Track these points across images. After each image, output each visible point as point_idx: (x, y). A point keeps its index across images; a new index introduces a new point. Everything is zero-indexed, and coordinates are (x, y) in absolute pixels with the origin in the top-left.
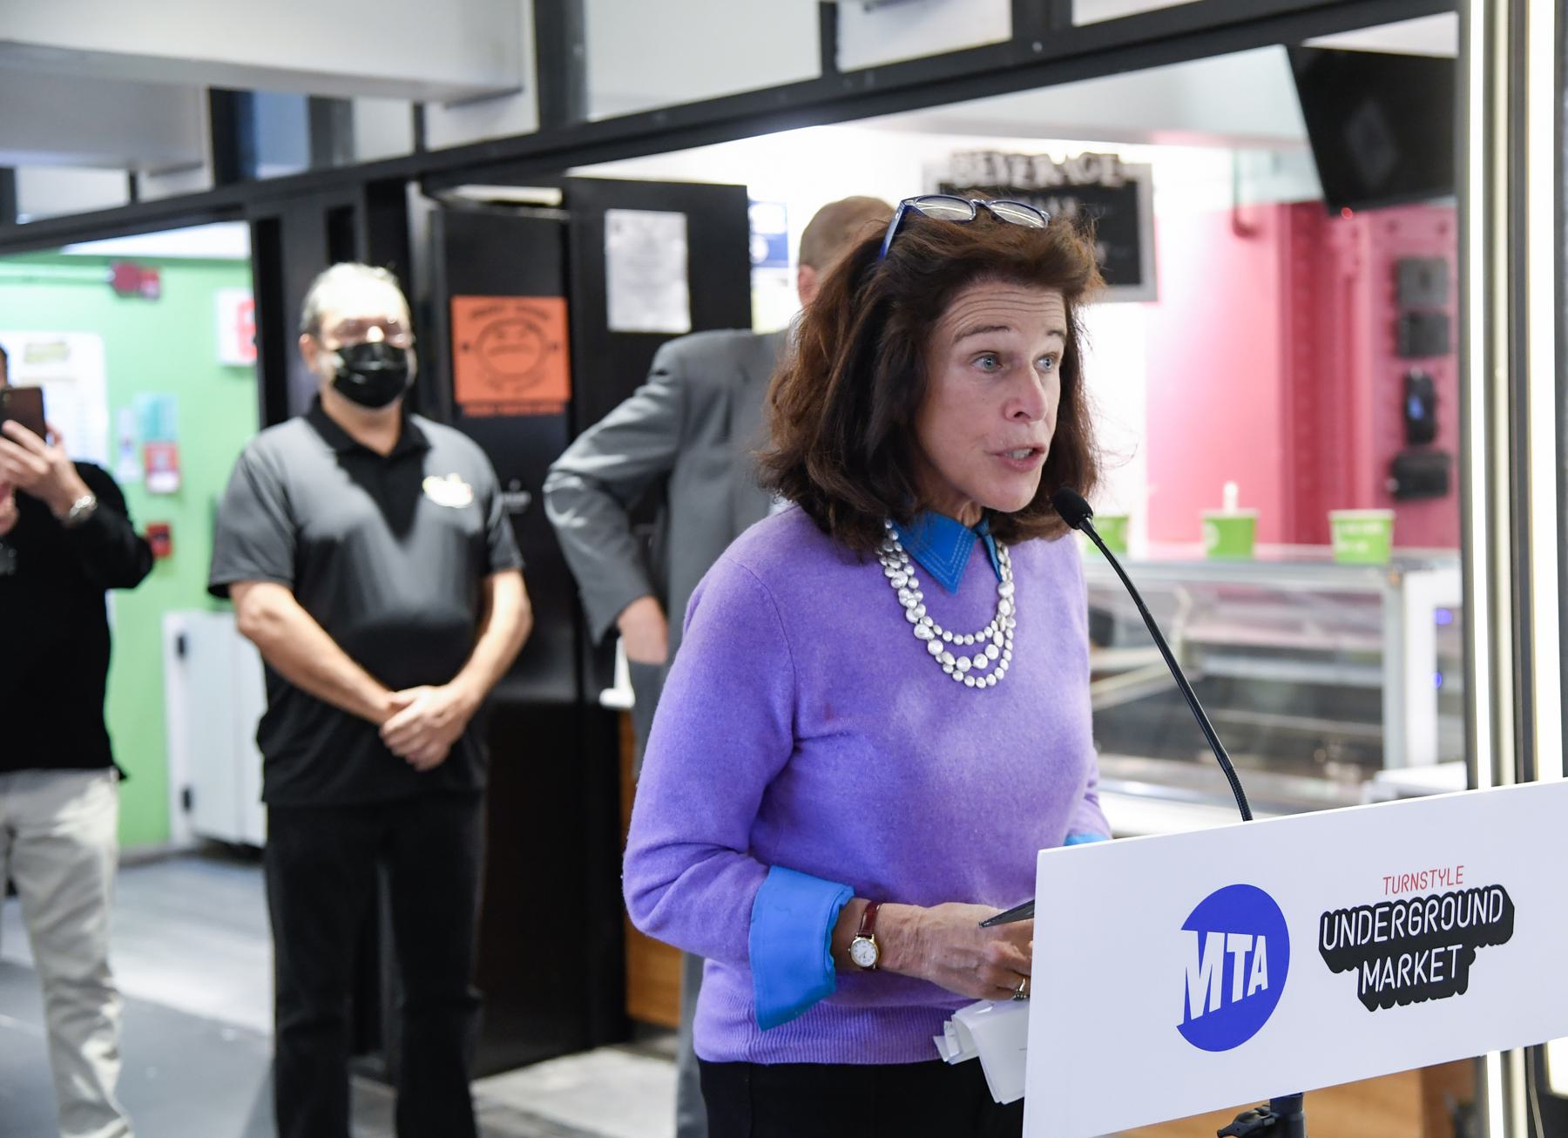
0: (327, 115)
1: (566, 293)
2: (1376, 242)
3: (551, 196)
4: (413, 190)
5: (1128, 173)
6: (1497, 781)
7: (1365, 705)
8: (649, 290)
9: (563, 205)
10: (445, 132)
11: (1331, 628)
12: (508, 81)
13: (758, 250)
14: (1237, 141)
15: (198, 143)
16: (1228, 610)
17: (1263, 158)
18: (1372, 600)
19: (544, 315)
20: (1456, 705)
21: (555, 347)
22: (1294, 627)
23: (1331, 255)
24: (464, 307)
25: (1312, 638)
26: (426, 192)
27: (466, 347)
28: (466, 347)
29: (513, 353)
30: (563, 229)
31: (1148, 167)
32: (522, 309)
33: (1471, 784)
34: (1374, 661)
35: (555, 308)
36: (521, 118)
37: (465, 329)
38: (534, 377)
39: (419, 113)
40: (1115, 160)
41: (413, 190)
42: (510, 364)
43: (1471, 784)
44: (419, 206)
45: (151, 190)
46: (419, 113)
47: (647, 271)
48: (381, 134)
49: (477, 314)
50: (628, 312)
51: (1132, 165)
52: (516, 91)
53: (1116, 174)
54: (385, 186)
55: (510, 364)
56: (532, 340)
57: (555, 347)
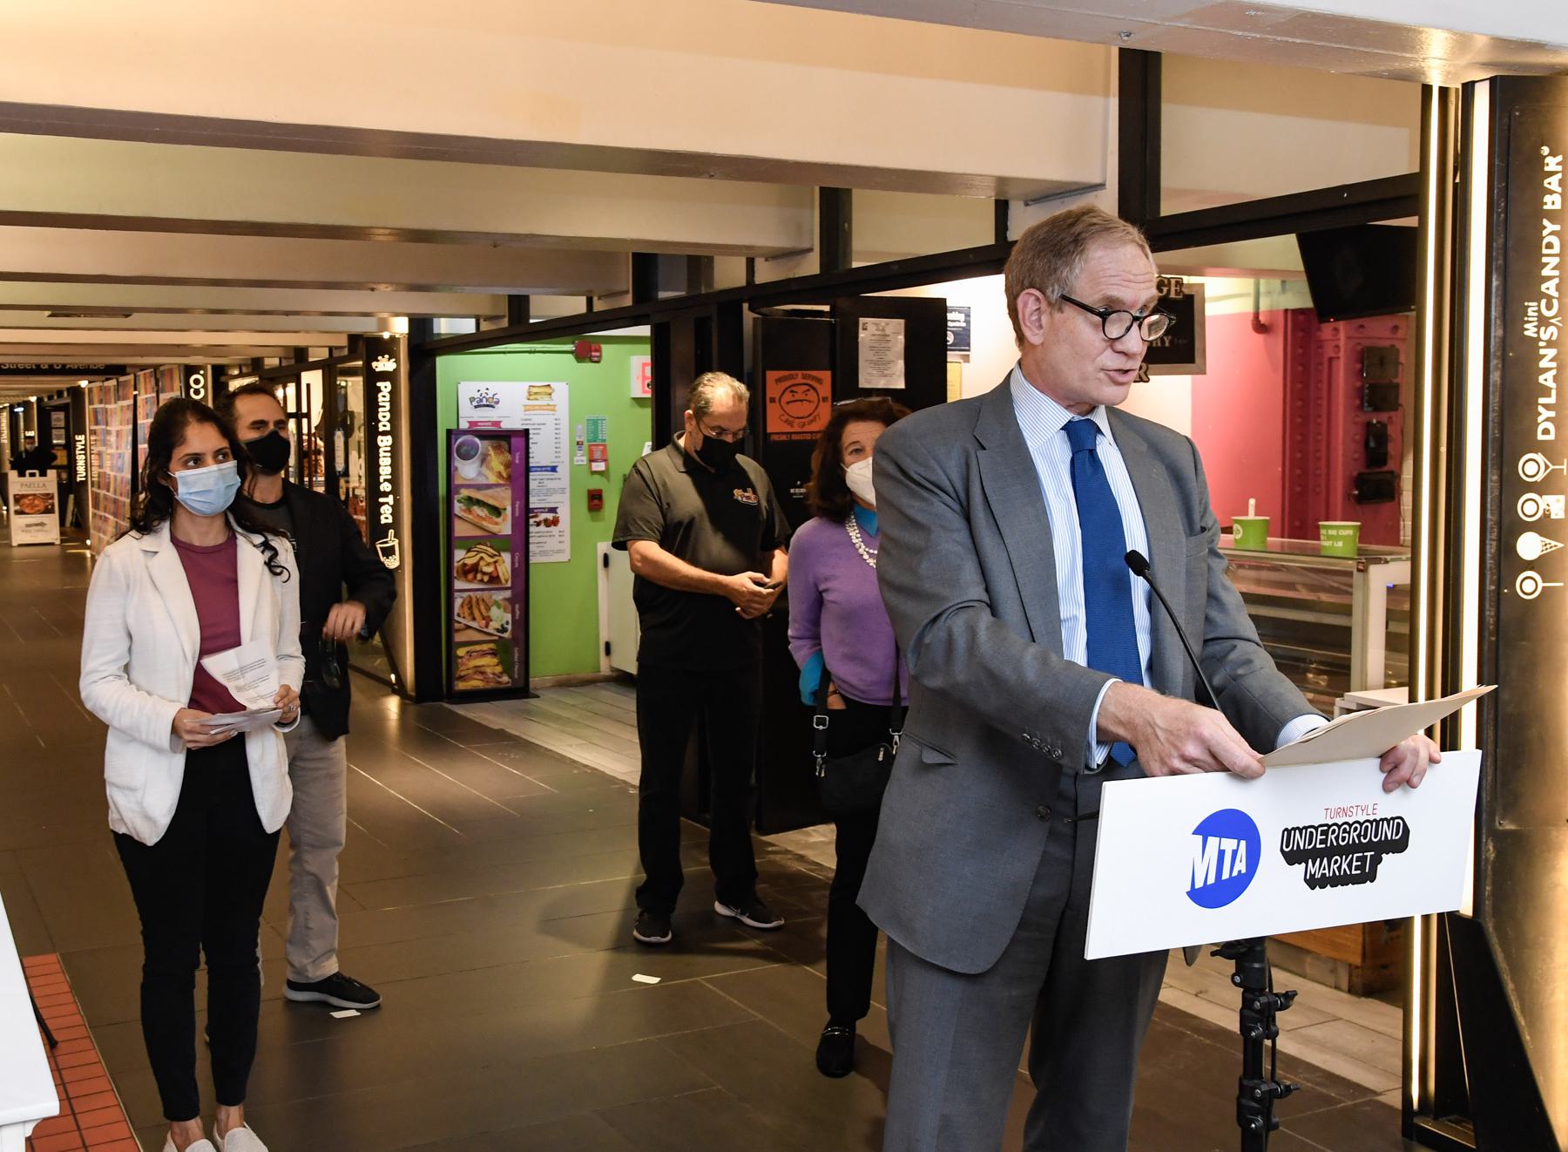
0: (698, 263)
1: (832, 367)
2: (1348, 338)
3: (826, 308)
4: (746, 306)
5: (1186, 291)
6: (1430, 696)
7: (1341, 639)
8: (882, 365)
9: (831, 314)
10: (766, 273)
11: (1312, 588)
12: (806, 245)
13: (950, 338)
14: (1257, 273)
15: (626, 280)
16: (1253, 574)
17: (1277, 282)
18: (1350, 574)
19: (819, 381)
20: (1400, 643)
21: (825, 399)
22: (1291, 586)
23: (1320, 345)
24: (772, 376)
25: (1303, 594)
26: (751, 309)
27: (773, 400)
28: (773, 400)
29: (800, 406)
30: (832, 326)
31: (1202, 285)
32: (804, 377)
33: (1412, 698)
34: (1347, 611)
35: (826, 375)
36: (811, 266)
37: (773, 390)
38: (812, 417)
39: (750, 263)
40: (1179, 283)
41: (746, 306)
42: (795, 410)
43: (1412, 698)
44: (748, 317)
45: (599, 306)
46: (750, 263)
47: (882, 355)
48: (730, 274)
49: (779, 380)
50: (869, 378)
51: (1190, 286)
52: (810, 250)
53: (1177, 293)
54: (730, 302)
55: (795, 410)
56: (812, 395)
57: (825, 399)
